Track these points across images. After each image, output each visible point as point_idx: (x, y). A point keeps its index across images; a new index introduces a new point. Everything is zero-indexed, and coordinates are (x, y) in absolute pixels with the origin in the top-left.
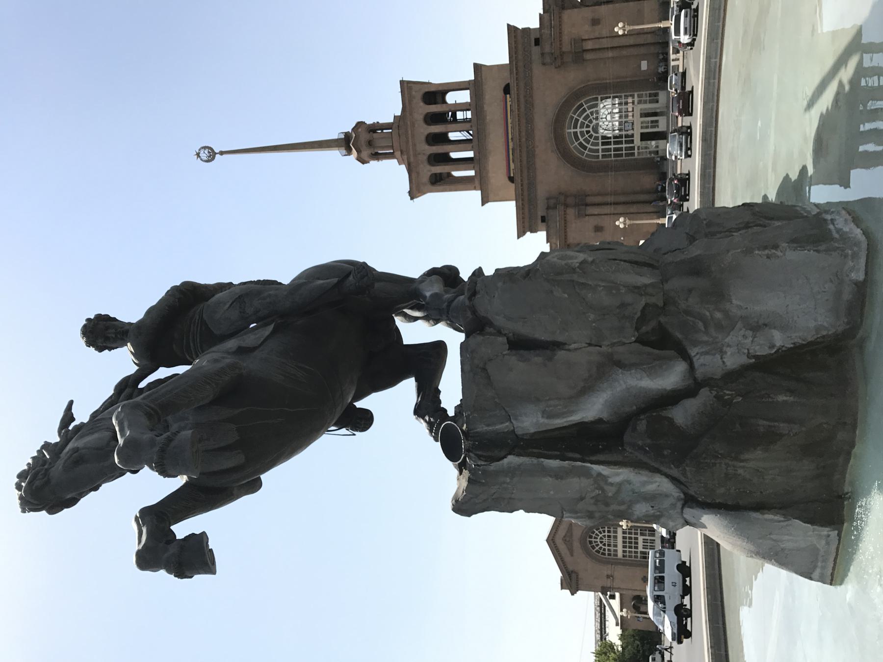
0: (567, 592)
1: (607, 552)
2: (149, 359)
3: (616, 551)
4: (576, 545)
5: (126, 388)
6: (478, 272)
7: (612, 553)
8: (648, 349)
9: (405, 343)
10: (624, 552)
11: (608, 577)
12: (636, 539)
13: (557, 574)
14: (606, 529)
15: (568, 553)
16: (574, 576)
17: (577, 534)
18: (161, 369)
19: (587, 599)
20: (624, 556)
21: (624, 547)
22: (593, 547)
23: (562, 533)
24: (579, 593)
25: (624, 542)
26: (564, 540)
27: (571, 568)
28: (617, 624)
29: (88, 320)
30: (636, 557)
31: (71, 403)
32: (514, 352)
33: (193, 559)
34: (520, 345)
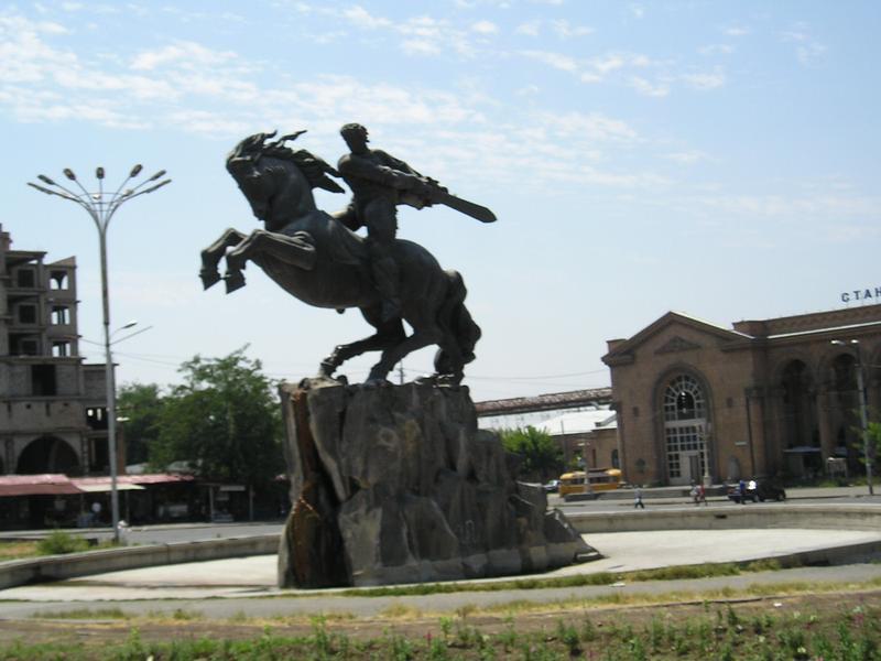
0: (605, 351)
1: (670, 404)
2: (346, 170)
3: (674, 419)
4: (672, 359)
5: (321, 166)
7: (670, 413)
10: (674, 430)
11: (636, 411)
12: (695, 447)
13: (628, 332)
14: (702, 401)
15: (658, 347)
16: (628, 357)
17: (689, 359)
18: (341, 179)
19: (602, 378)
20: (668, 430)
21: (681, 429)
22: (673, 383)
23: (685, 334)
24: (607, 367)
25: (687, 429)
26: (675, 340)
27: (639, 353)
28: (598, 424)
30: (670, 449)
31: (304, 132)
33: (209, 277)
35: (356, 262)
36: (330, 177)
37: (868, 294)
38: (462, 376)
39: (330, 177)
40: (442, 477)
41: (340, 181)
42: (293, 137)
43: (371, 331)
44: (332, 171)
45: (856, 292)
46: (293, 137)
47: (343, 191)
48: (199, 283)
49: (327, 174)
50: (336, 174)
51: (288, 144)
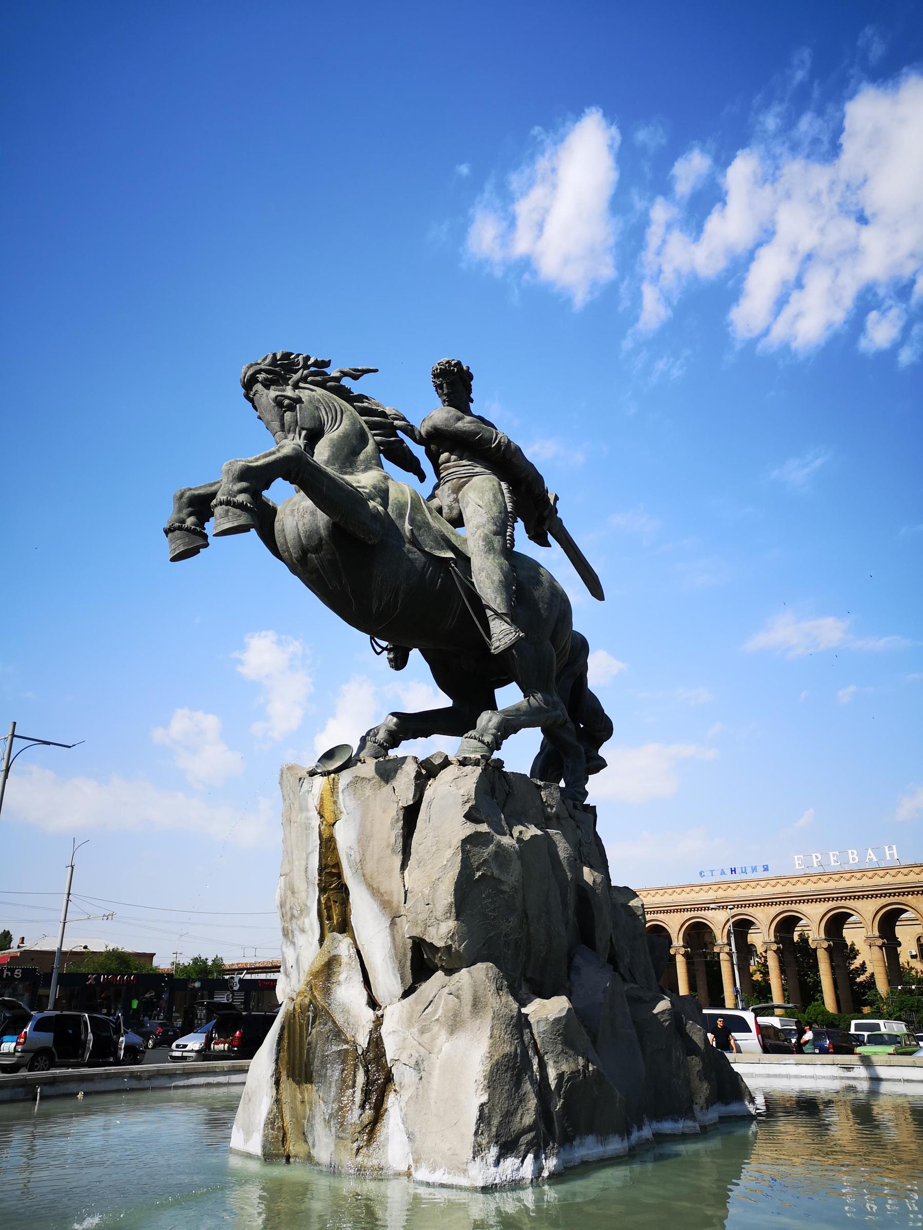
6: (601, 764)
8: (409, 955)
9: (496, 691)
29: (459, 364)
31: (376, 371)
32: (401, 813)
34: (411, 815)
35: (450, 555)
36: (409, 442)
37: (723, 873)
38: (586, 794)
39: (409, 442)
40: (578, 960)
41: (419, 451)
42: (356, 375)
43: (443, 701)
44: (410, 430)
45: (712, 871)
46: (356, 375)
47: (422, 477)
48: (166, 547)
49: (399, 432)
50: (420, 441)
51: (347, 382)
